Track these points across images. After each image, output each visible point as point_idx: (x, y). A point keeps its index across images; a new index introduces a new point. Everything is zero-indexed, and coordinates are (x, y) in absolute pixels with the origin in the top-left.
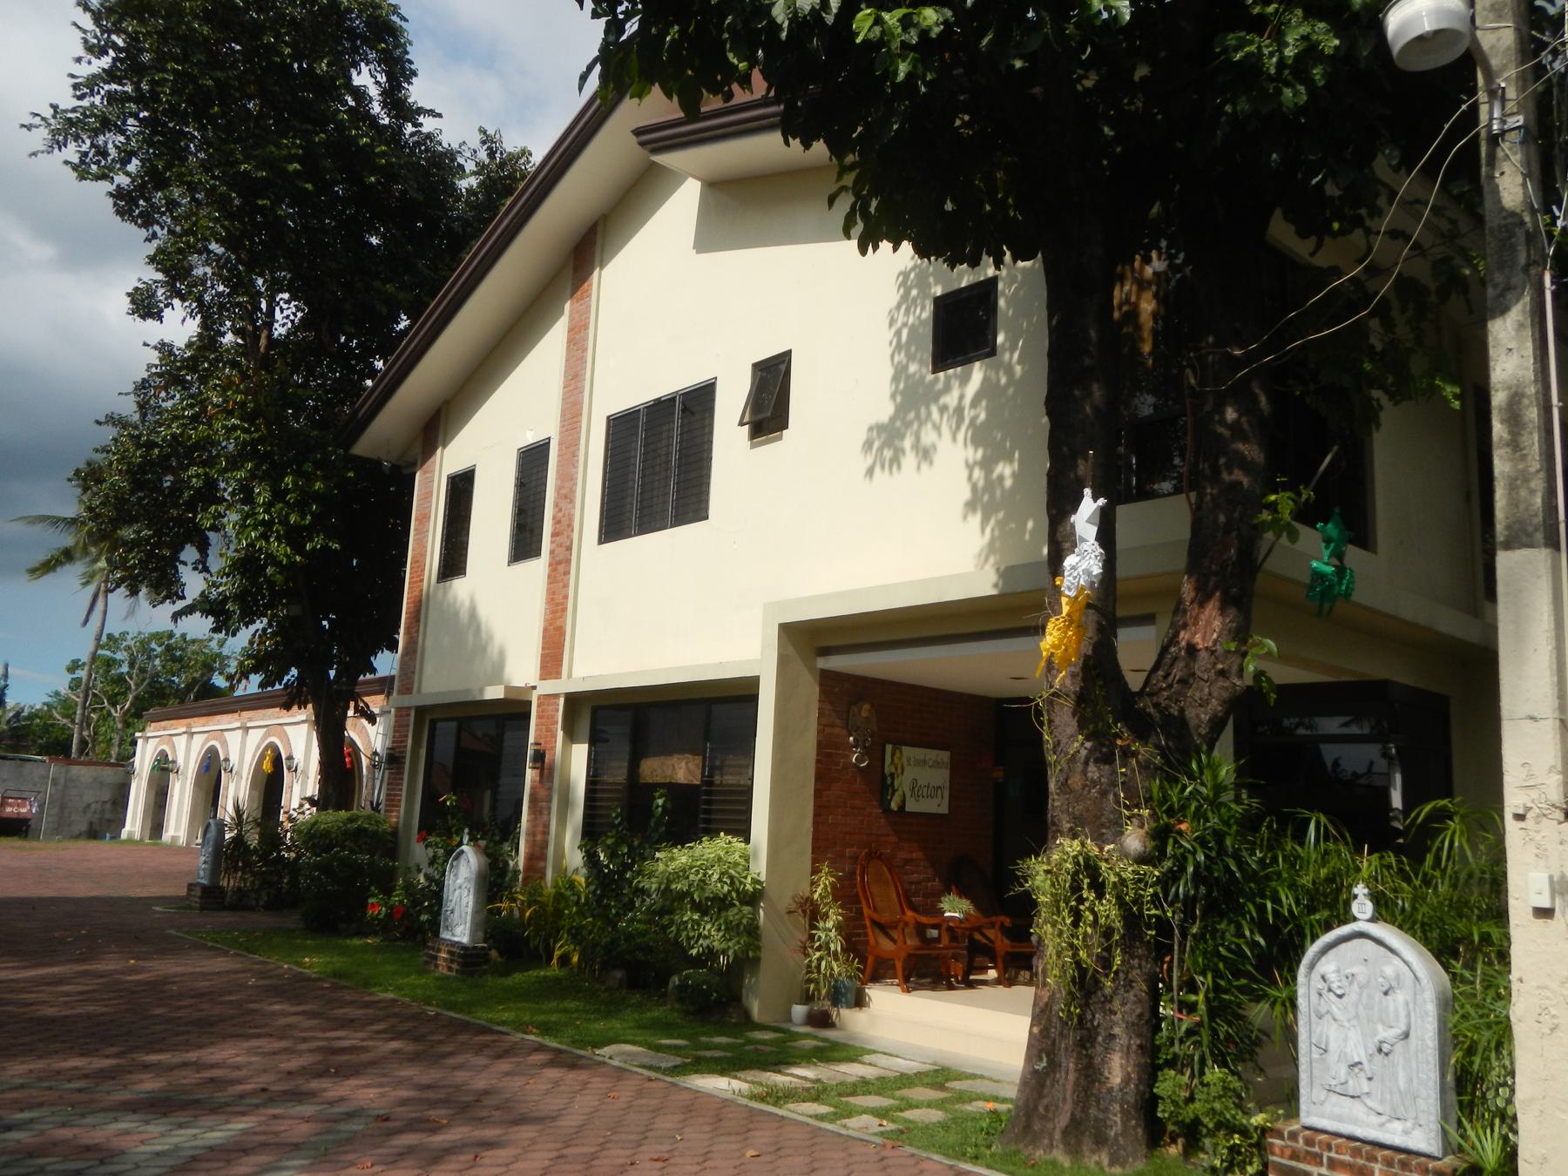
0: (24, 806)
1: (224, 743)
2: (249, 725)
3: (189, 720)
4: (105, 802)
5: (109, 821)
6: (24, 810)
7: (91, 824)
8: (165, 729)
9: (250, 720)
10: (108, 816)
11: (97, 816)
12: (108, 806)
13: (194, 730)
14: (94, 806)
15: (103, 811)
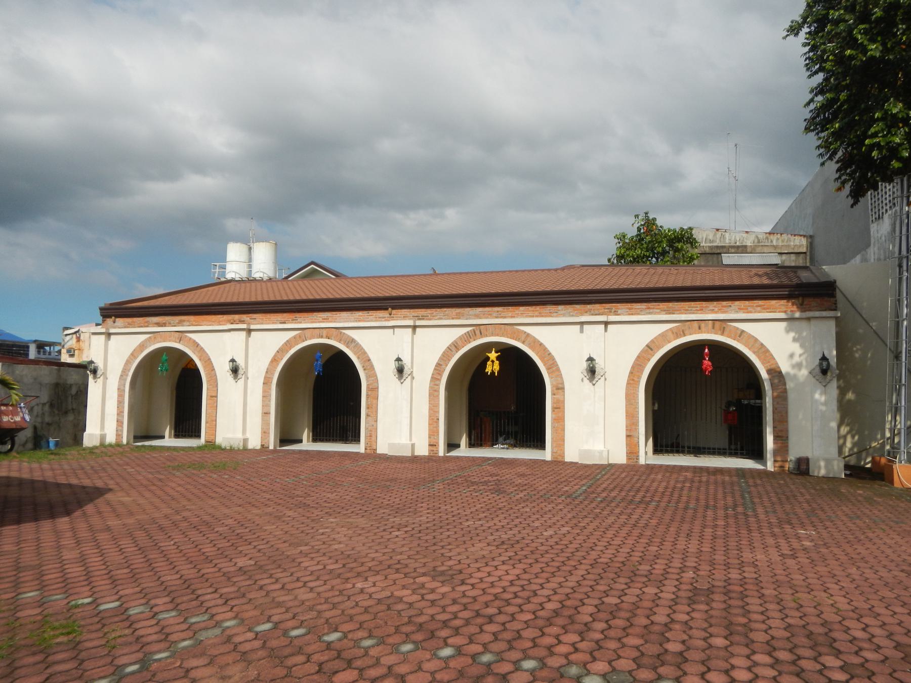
0: (17, 414)
1: (351, 342)
2: (418, 323)
3: (237, 317)
4: (44, 404)
5: (48, 424)
6: (18, 419)
7: (35, 428)
8: (158, 324)
9: (422, 318)
10: (47, 419)
11: (39, 420)
12: (47, 408)
13: (252, 327)
14: (36, 408)
15: (43, 414)
